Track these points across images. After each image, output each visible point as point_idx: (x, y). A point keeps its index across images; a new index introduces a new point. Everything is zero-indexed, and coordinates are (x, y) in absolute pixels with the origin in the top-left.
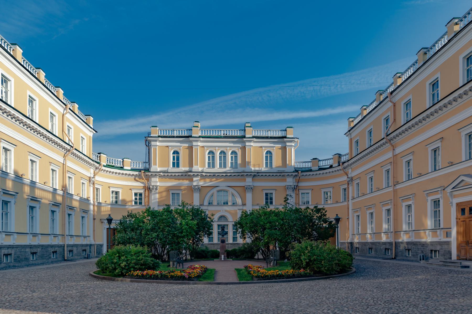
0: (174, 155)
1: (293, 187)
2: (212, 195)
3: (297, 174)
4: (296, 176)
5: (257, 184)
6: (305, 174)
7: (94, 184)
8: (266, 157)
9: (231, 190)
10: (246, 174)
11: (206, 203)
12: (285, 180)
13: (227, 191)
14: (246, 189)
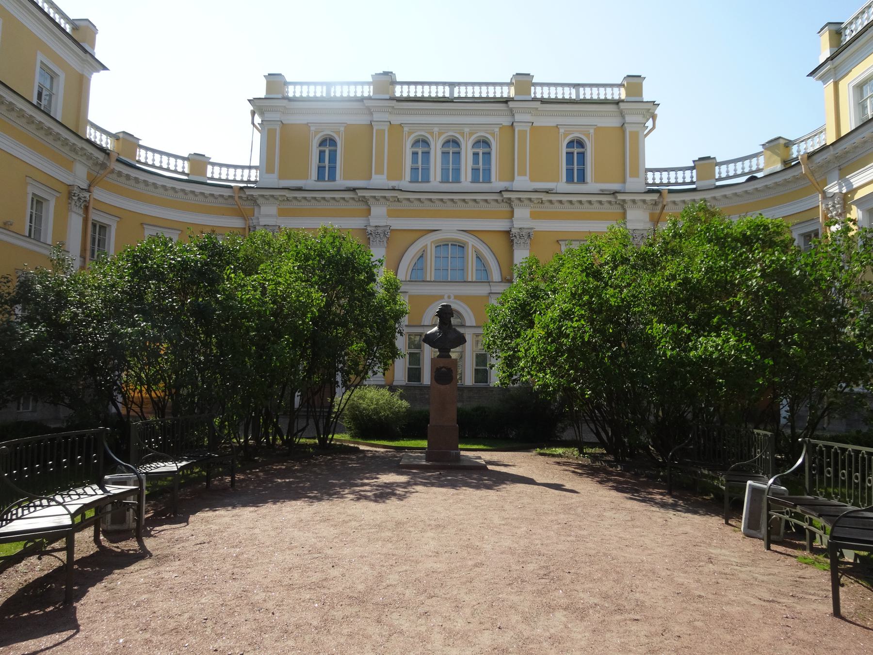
0: (322, 148)
3: (655, 197)
7: (86, 208)
8: (570, 155)
9: (471, 242)
13: (462, 246)
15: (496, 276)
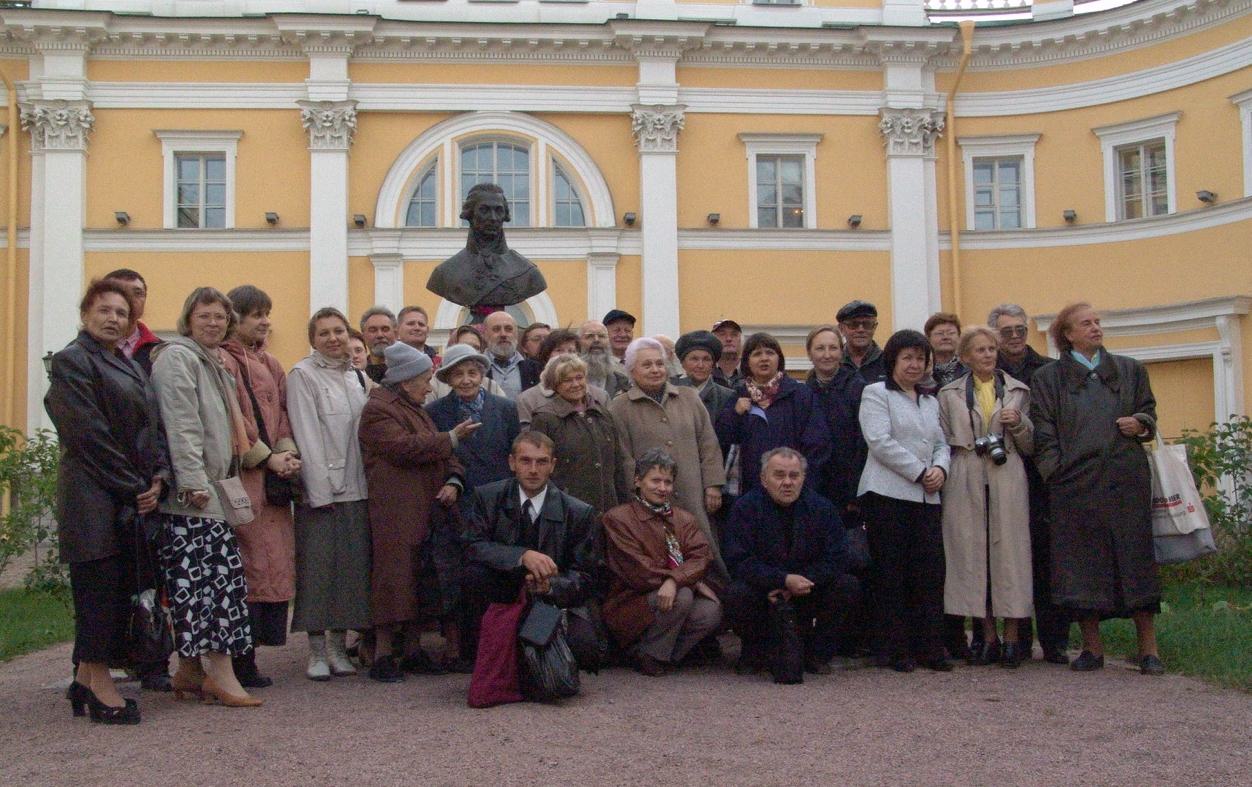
1: (927, 118)
2: (428, 173)
4: (943, 52)
5: (705, 100)
6: (995, 41)
9: (544, 140)
10: (637, 33)
11: (388, 214)
12: (877, 80)
14: (631, 129)
15: (602, 214)
